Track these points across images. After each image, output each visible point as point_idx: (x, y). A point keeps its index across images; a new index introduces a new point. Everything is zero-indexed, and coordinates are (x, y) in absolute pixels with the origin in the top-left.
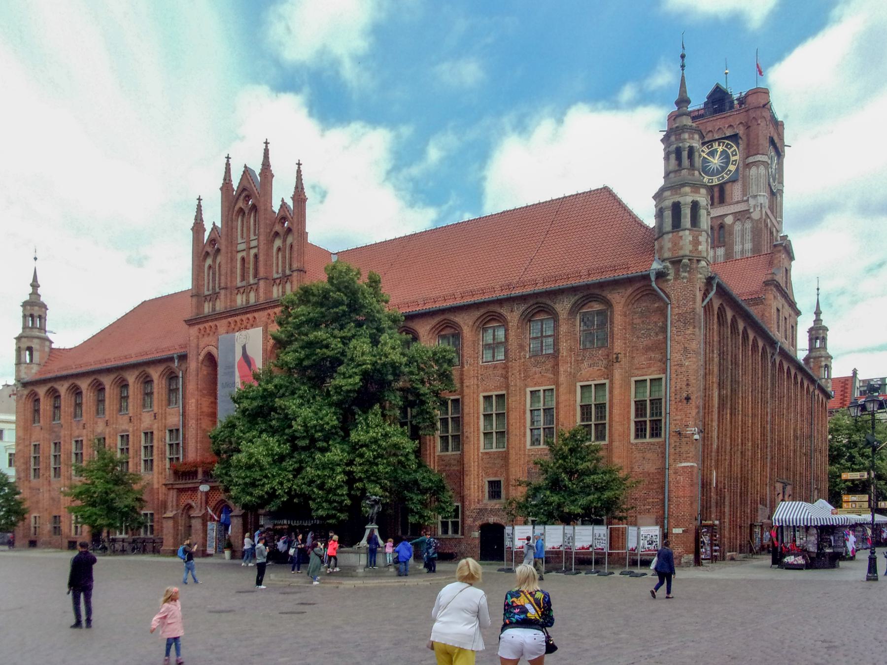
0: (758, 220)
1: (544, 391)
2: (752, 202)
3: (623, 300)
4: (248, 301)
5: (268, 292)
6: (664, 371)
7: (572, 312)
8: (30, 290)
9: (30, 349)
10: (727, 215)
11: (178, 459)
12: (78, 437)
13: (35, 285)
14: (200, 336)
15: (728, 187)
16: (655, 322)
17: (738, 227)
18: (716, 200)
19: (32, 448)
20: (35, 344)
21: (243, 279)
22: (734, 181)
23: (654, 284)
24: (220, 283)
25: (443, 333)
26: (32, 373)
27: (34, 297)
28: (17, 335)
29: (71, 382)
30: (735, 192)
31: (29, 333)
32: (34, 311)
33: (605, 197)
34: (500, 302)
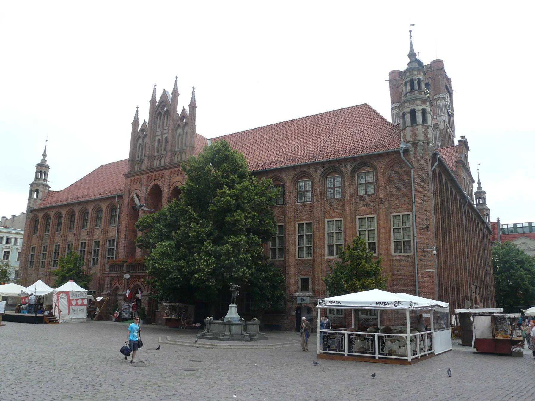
0: (443, 129)
3: (383, 167)
4: (160, 164)
6: (411, 210)
8: (42, 158)
9: (37, 191)
11: (113, 258)
12: (58, 243)
13: (44, 155)
14: (132, 184)
19: (31, 249)
20: (41, 189)
21: (158, 152)
24: (145, 153)
26: (38, 204)
27: (43, 161)
28: (31, 183)
31: (38, 182)
32: (42, 169)
34: (308, 165)
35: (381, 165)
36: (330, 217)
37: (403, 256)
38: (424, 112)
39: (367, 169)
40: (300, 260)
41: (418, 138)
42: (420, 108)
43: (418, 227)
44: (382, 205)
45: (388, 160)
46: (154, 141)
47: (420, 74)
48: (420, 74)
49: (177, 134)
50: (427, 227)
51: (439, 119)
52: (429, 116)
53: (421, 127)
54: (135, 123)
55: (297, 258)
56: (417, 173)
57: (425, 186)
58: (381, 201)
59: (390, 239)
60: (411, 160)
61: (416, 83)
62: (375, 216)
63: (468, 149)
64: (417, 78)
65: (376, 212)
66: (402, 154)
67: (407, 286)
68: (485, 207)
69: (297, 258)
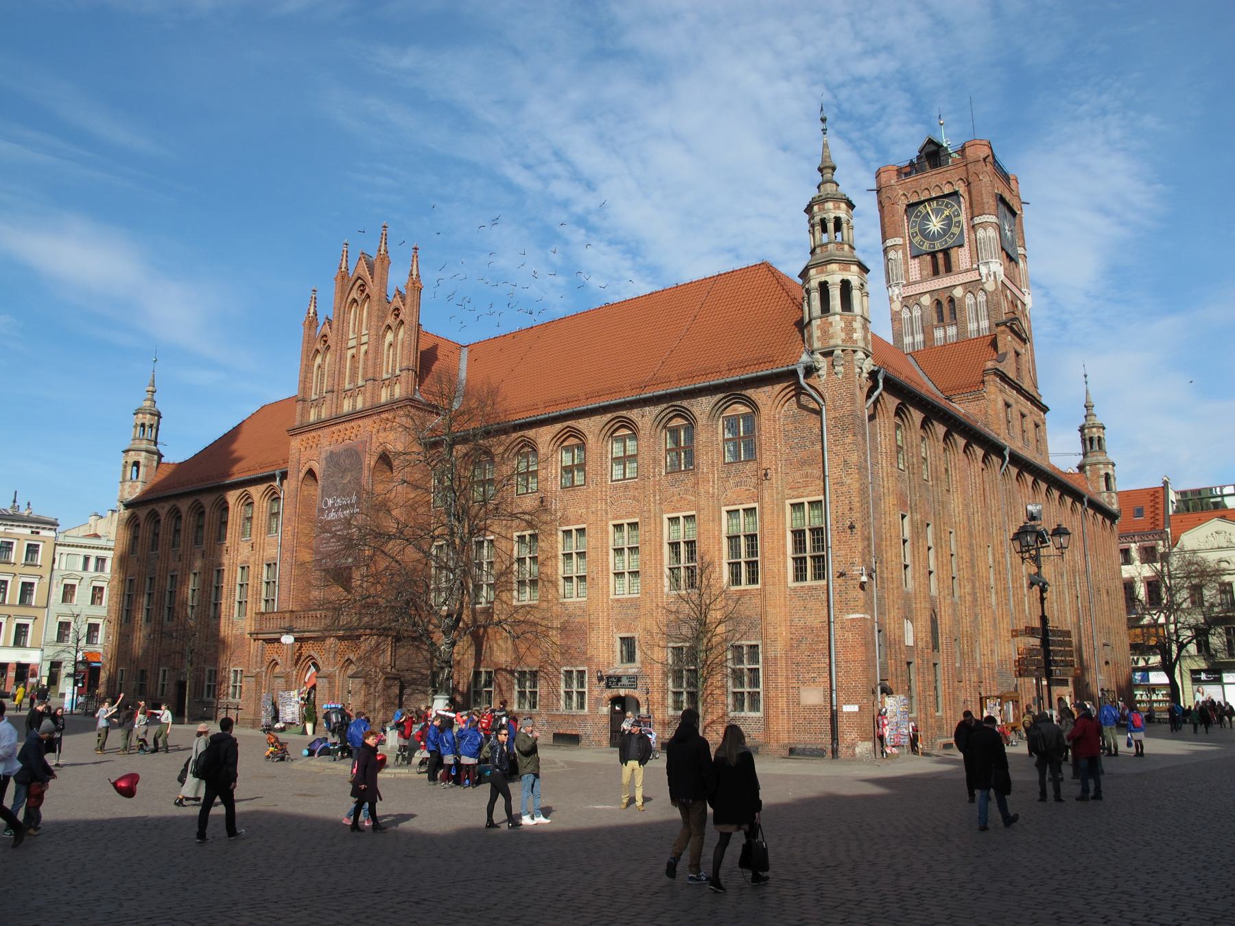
2: (983, 270)
5: (375, 394)
7: (712, 416)
15: (953, 252)
16: (810, 428)
17: (969, 300)
18: (942, 268)
22: (961, 246)
23: (802, 381)
25: (565, 444)
29: (171, 503)
30: (962, 257)
36: (674, 510)
37: (809, 587)
38: (846, 286)
40: (618, 600)
41: (832, 342)
43: (835, 527)
46: (342, 358)
47: (839, 208)
48: (839, 208)
49: (386, 344)
50: (852, 527)
52: (856, 294)
53: (838, 317)
54: (312, 322)
55: (612, 597)
56: (832, 414)
57: (848, 441)
58: (766, 475)
59: (785, 554)
60: (821, 389)
64: (832, 216)
65: (759, 498)
66: (801, 376)
67: (817, 650)
68: (1101, 458)
69: (612, 597)
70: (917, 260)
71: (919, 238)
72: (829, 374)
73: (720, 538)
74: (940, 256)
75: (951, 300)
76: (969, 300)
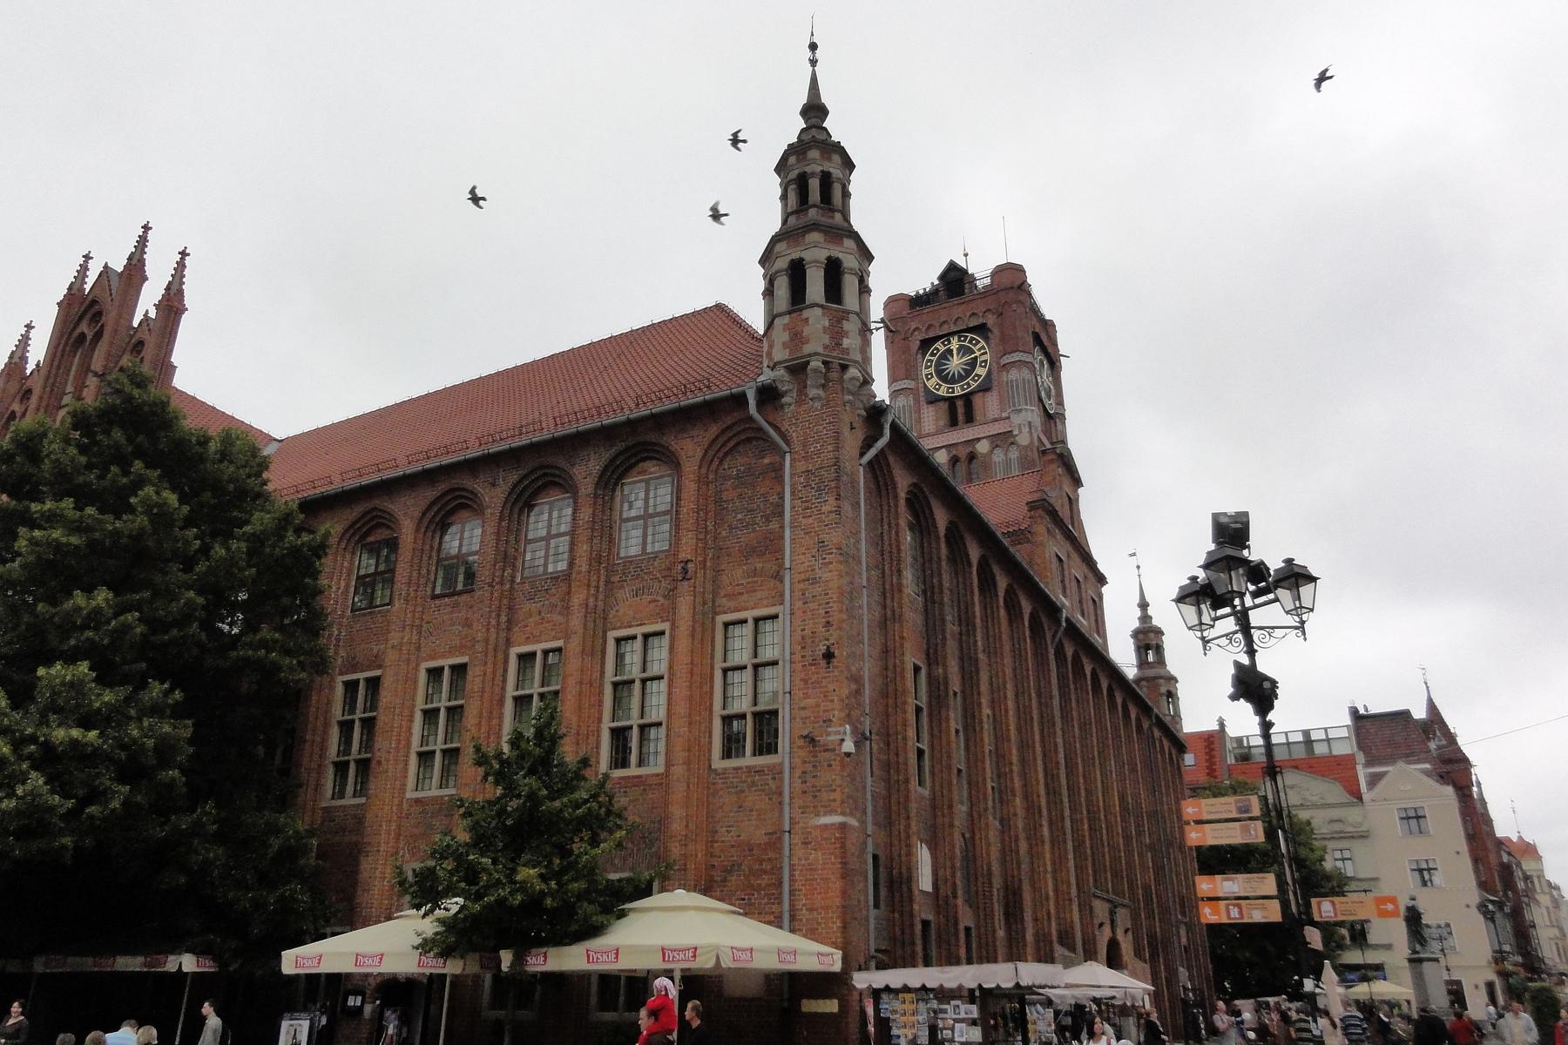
1: (546, 653)
3: (699, 454)
10: (979, 439)
15: (977, 400)
30: (989, 405)
33: (721, 314)
35: (690, 447)
36: (528, 641)
39: (652, 468)
40: (418, 801)
42: (822, 254)
43: (798, 657)
44: (685, 583)
45: (714, 430)
47: (829, 159)
50: (829, 656)
51: (1017, 419)
53: (818, 311)
56: (801, 466)
57: (826, 508)
58: (685, 571)
60: (785, 426)
61: (814, 185)
62: (666, 626)
63: (1077, 482)
65: (669, 614)
69: (409, 795)
70: (931, 408)
71: (935, 379)
72: (799, 402)
73: (601, 685)
74: (960, 404)
75: (972, 457)
76: (998, 456)
